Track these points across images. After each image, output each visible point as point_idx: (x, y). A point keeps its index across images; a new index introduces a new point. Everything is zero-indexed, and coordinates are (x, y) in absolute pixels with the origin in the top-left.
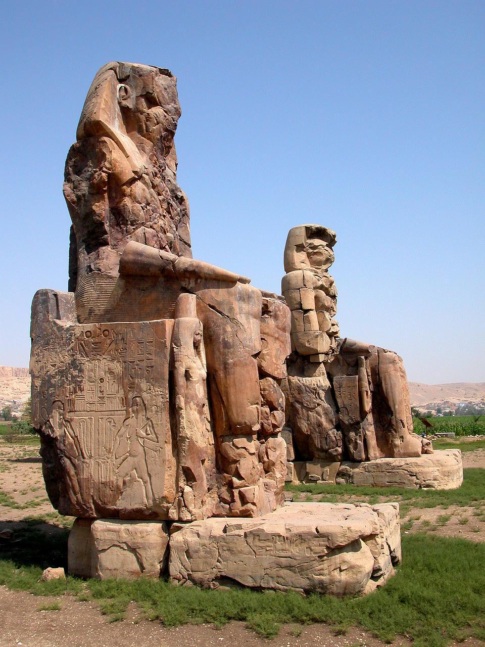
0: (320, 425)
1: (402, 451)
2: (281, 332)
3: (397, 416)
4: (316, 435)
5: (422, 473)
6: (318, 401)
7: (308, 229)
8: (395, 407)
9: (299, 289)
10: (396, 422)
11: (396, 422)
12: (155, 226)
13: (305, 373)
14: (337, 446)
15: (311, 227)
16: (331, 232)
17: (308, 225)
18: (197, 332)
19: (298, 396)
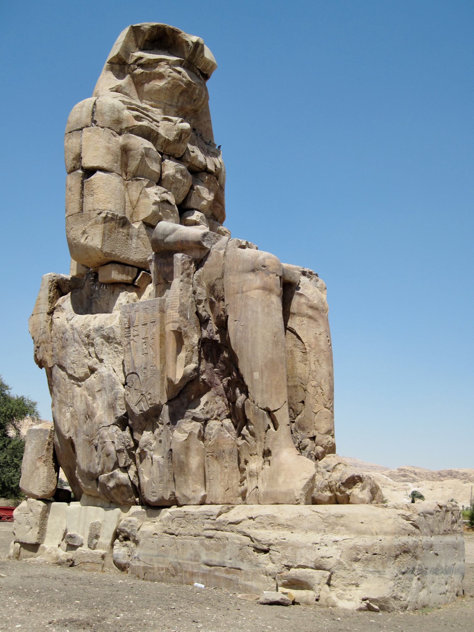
1: (262, 489)
3: (258, 399)
5: (283, 544)
6: (92, 362)
8: (252, 376)
9: (81, 129)
11: (255, 414)
13: (94, 308)
14: (116, 465)
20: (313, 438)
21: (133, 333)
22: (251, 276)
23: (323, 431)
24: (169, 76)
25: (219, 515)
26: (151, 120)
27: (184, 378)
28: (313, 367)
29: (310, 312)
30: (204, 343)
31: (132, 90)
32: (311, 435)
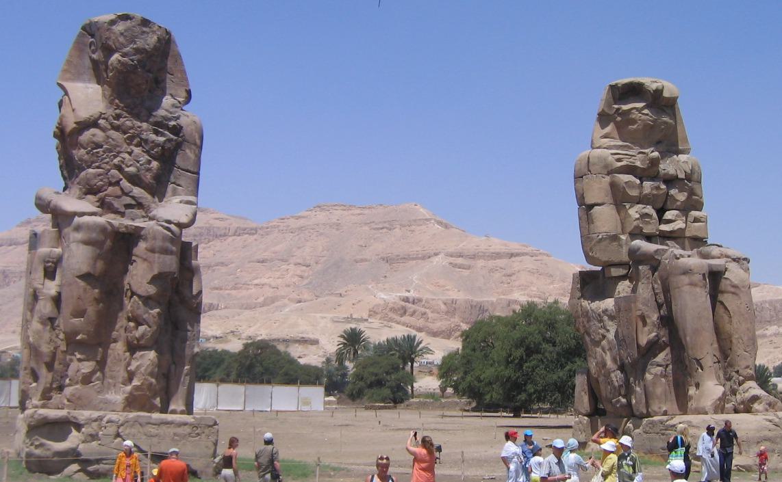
0: (604, 365)
2: (150, 254)
3: (690, 352)
4: (601, 379)
6: (602, 331)
7: (613, 88)
8: (686, 340)
10: (690, 361)
11: (690, 361)
12: (103, 166)
14: (620, 395)
15: (616, 84)
16: (651, 83)
17: (613, 83)
18: (47, 259)
19: (587, 326)
20: (737, 372)
21: (621, 315)
22: (683, 277)
23: (743, 367)
24: (640, 120)
25: (667, 421)
26: (629, 157)
27: (648, 343)
28: (735, 326)
29: (733, 290)
30: (661, 318)
31: (615, 134)
32: (736, 370)
